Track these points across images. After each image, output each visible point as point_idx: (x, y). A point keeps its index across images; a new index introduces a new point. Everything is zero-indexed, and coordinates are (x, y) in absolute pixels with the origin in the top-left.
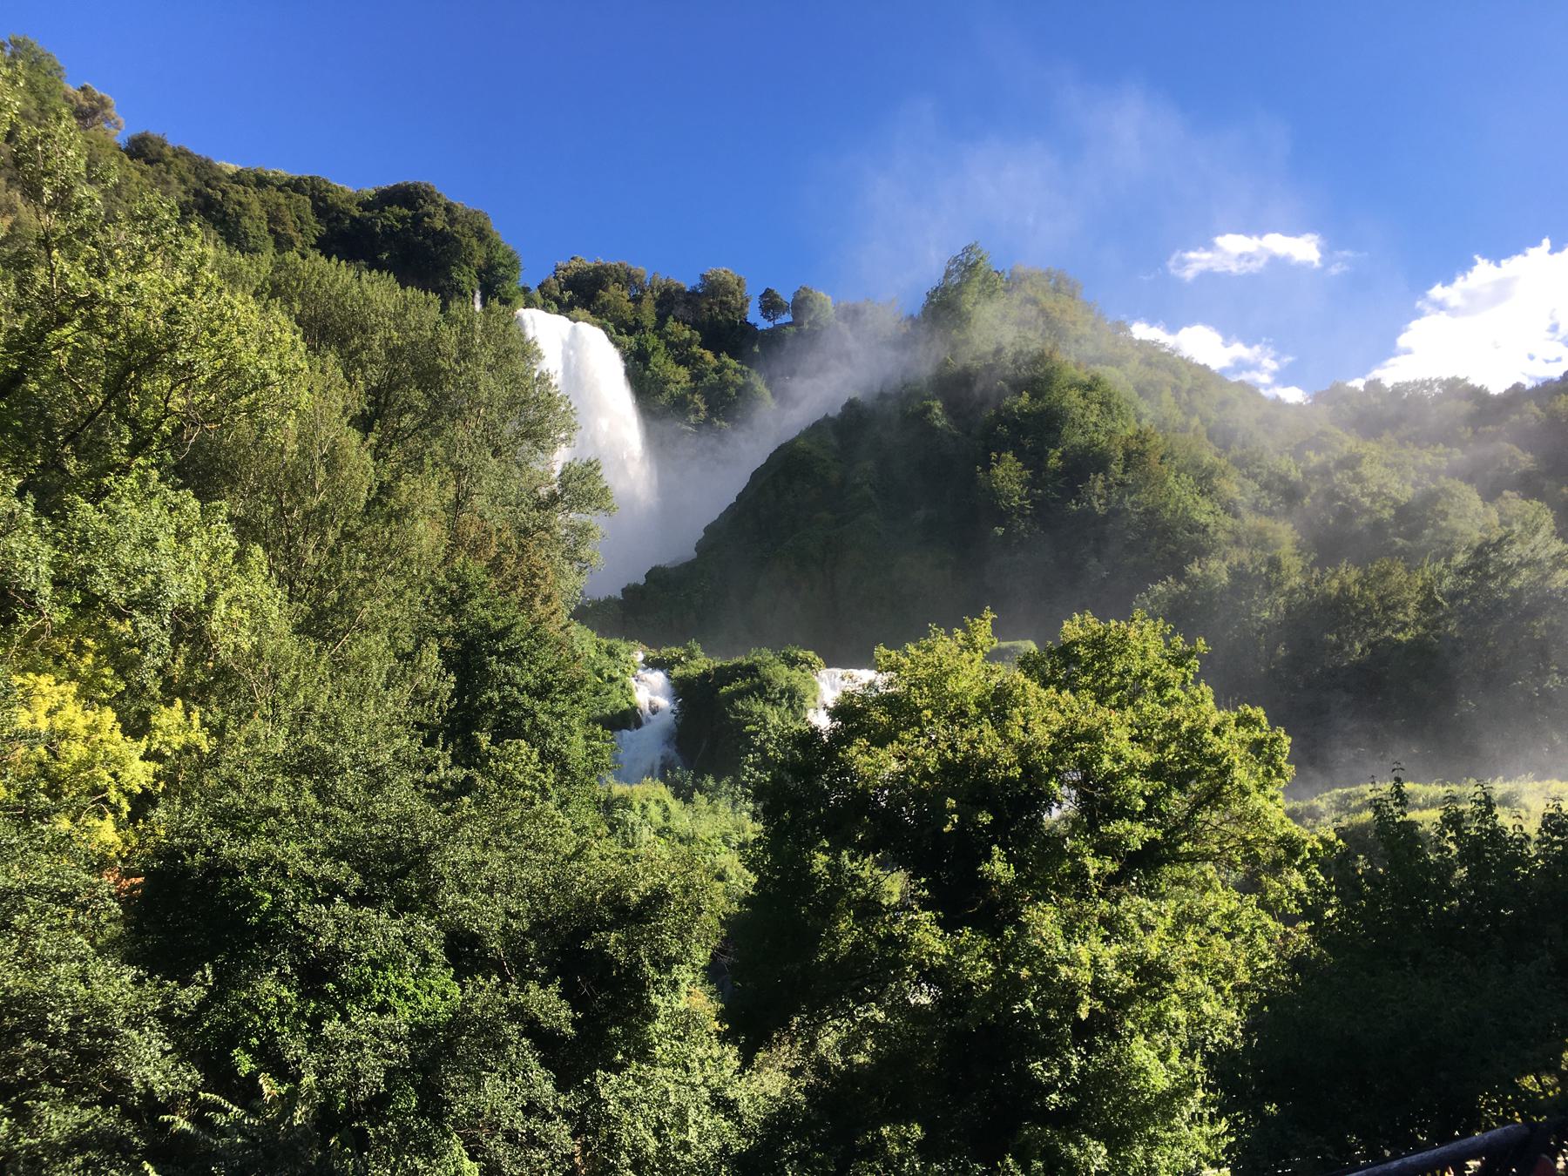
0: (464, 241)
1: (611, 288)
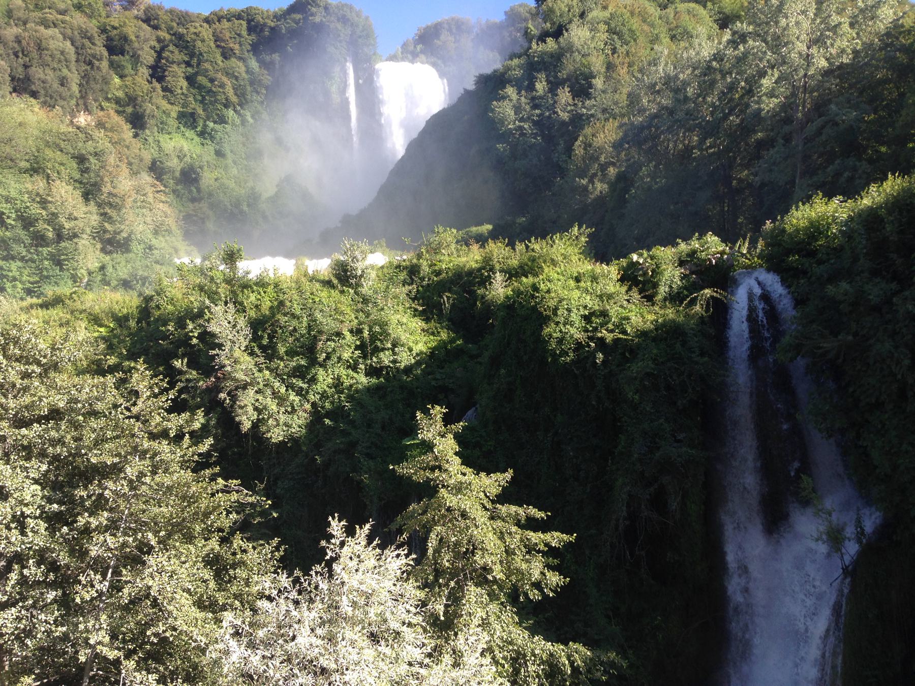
0: (332, 26)
1: (443, 37)
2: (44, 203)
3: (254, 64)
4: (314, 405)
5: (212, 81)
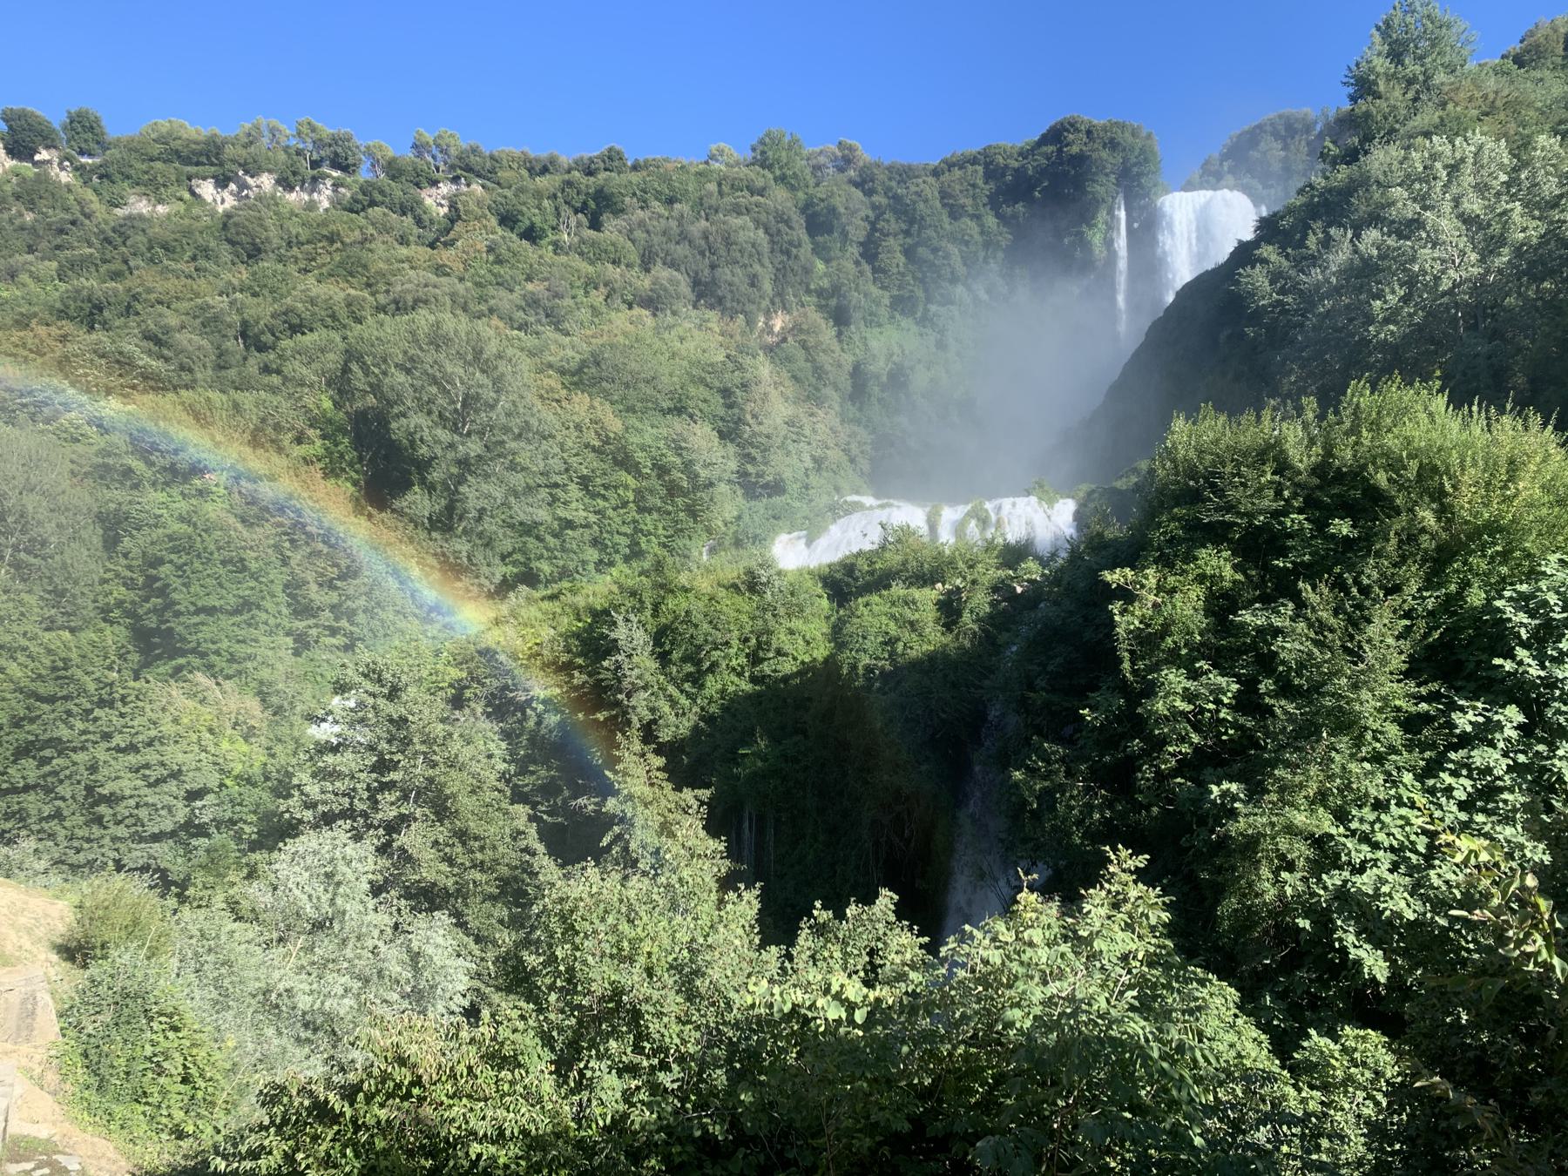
0: (1095, 155)
2: (679, 450)
3: (991, 221)
4: (702, 709)
5: (935, 250)
